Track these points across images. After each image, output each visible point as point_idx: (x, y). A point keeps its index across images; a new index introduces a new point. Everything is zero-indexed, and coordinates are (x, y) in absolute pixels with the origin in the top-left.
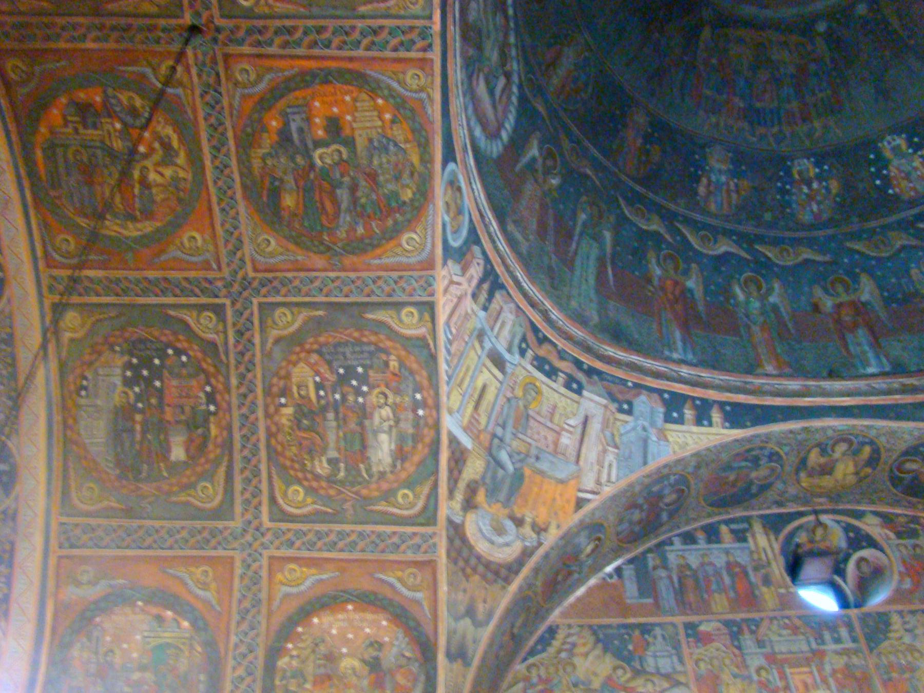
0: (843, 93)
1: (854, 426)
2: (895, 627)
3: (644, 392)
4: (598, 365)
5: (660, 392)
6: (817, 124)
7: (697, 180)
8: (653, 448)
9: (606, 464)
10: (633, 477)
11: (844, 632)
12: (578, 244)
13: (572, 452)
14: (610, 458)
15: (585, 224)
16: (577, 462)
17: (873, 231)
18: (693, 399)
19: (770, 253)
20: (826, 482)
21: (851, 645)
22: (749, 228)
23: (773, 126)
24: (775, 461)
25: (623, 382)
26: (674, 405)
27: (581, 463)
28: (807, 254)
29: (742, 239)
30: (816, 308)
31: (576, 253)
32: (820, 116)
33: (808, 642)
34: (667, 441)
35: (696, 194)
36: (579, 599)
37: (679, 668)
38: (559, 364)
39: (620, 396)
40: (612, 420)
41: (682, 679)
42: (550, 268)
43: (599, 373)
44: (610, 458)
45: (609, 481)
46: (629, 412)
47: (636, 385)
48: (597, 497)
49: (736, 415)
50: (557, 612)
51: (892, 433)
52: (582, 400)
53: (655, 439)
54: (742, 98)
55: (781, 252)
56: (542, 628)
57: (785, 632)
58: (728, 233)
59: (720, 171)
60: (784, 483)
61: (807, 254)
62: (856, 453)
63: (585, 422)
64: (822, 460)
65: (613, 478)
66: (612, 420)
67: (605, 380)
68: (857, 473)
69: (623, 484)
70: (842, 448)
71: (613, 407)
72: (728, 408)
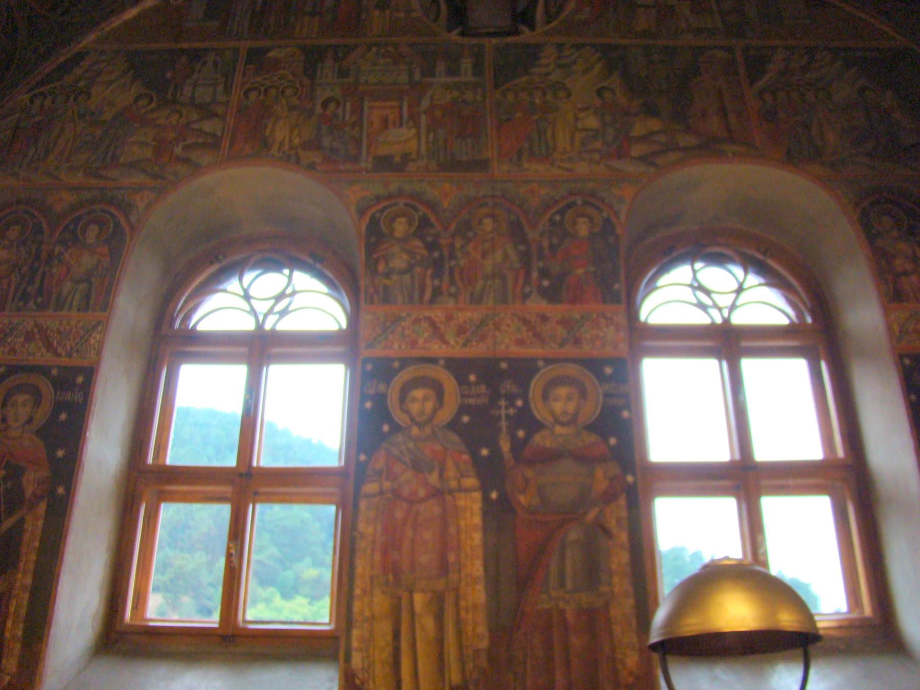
2: (544, 61)
11: (467, 64)
21: (470, 78)
33: (411, 74)
36: (125, 23)
37: (221, 98)
41: (220, 110)
50: (92, 37)
56: (64, 55)
57: (382, 61)
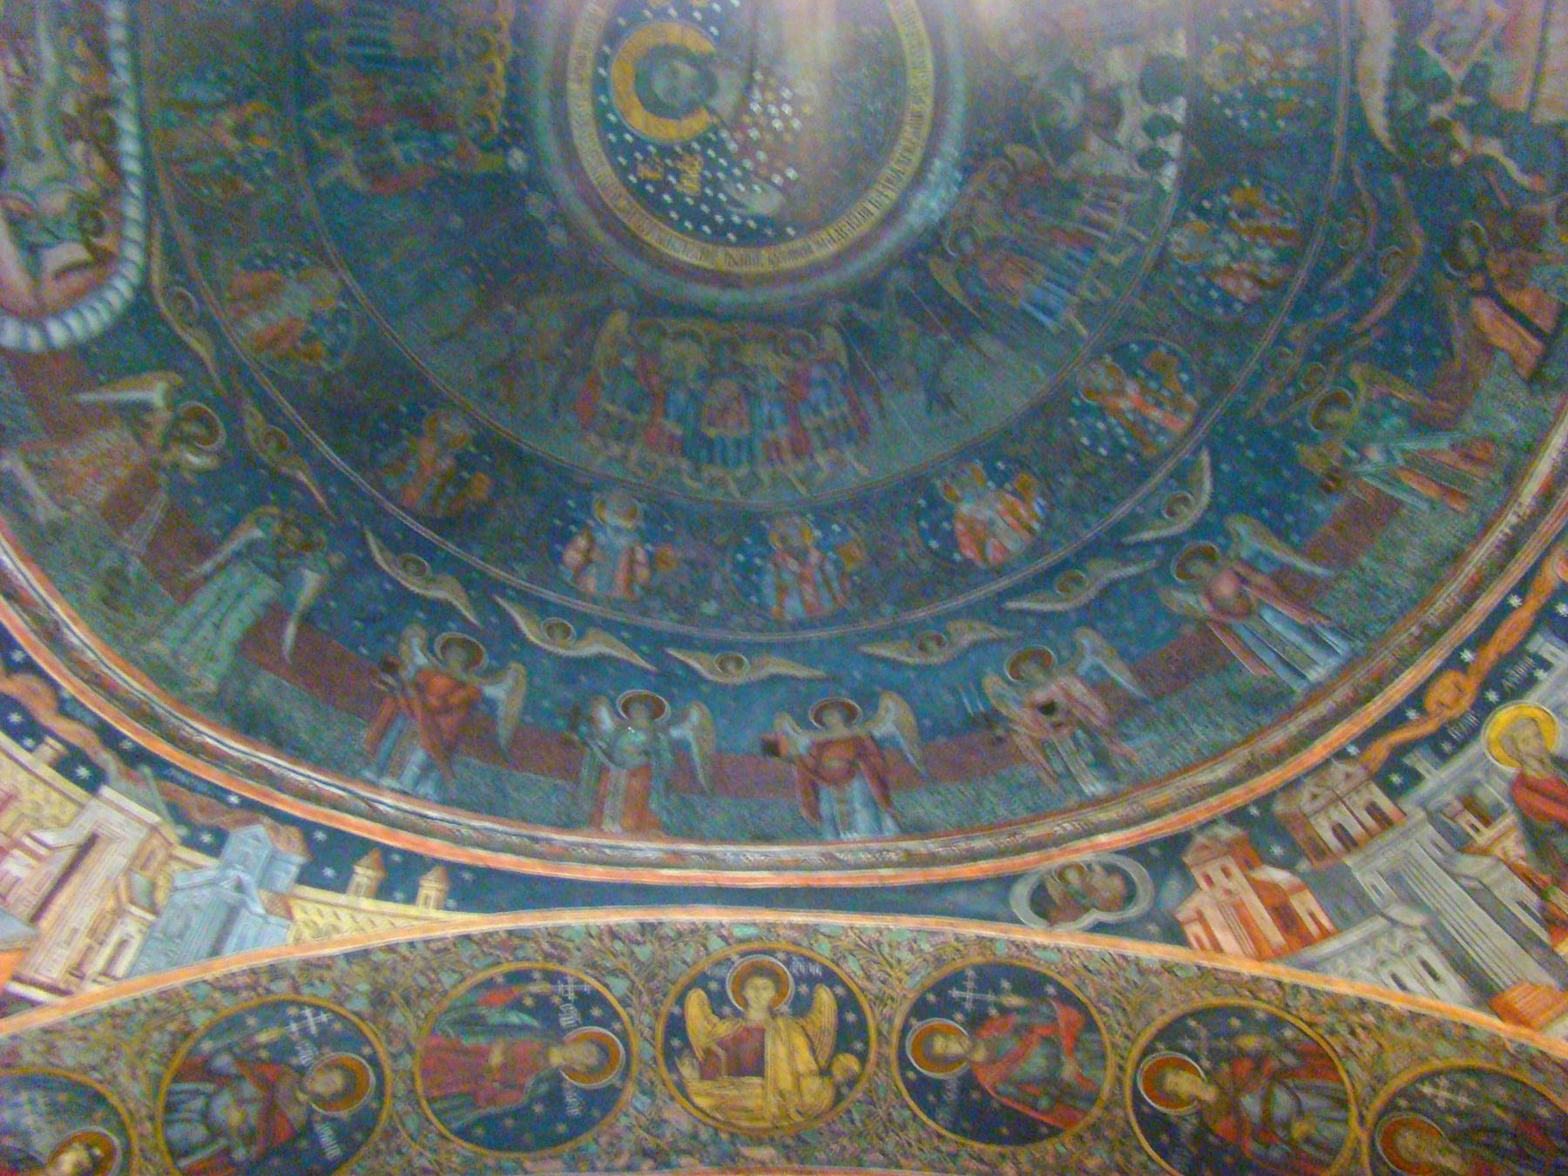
0: (869, 405)
1: (771, 927)
3: (267, 820)
4: (163, 749)
5: (306, 828)
6: (822, 459)
7: (566, 539)
8: (246, 925)
9: (114, 939)
10: (178, 979)
12: (220, 568)
13: (25, 898)
14: (132, 927)
15: (253, 546)
16: (35, 918)
17: (921, 625)
18: (387, 850)
19: (699, 663)
20: (751, 1093)
22: (666, 623)
23: (738, 462)
24: (599, 1022)
25: (219, 793)
26: (329, 859)
27: (45, 924)
28: (778, 666)
29: (636, 637)
30: (772, 748)
31: (207, 578)
32: (826, 446)
34: (289, 915)
35: (558, 559)
38: (47, 717)
39: (199, 818)
40: (160, 856)
42: (118, 574)
43: (160, 767)
44: (132, 927)
45: (105, 973)
46: (214, 850)
47: (247, 804)
48: (62, 1000)
49: (472, 888)
51: (870, 947)
52: (94, 803)
53: (260, 910)
54: (680, 420)
55: (722, 665)
58: (609, 626)
59: (618, 530)
60: (648, 1092)
61: (778, 666)
62: (802, 1007)
63: (88, 846)
64: (724, 1029)
65: (121, 969)
66: (160, 856)
67: (172, 779)
68: (825, 1072)
69: (145, 987)
70: (760, 994)
71: (173, 833)
72: (467, 876)
